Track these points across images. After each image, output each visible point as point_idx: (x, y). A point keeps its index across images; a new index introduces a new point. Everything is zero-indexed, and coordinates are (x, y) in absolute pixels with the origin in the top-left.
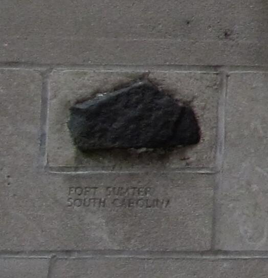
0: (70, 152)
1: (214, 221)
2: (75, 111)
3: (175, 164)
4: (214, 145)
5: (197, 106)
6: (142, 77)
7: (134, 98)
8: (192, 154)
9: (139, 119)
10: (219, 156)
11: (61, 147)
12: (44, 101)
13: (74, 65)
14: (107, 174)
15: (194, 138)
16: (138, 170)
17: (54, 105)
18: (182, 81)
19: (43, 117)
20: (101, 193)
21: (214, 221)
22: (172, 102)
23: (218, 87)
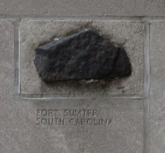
0: (36, 82)
1: (145, 135)
2: (39, 51)
3: (114, 91)
4: (142, 77)
5: (128, 48)
6: (87, 25)
7: (83, 41)
8: (126, 84)
9: (87, 58)
10: (147, 86)
11: (30, 78)
12: (16, 43)
13: (37, 16)
14: (64, 99)
15: (127, 72)
16: (87, 96)
17: (22, 47)
18: (116, 28)
19: (16, 56)
20: (61, 114)
21: (145, 135)
22: (110, 45)
23: (143, 32)
